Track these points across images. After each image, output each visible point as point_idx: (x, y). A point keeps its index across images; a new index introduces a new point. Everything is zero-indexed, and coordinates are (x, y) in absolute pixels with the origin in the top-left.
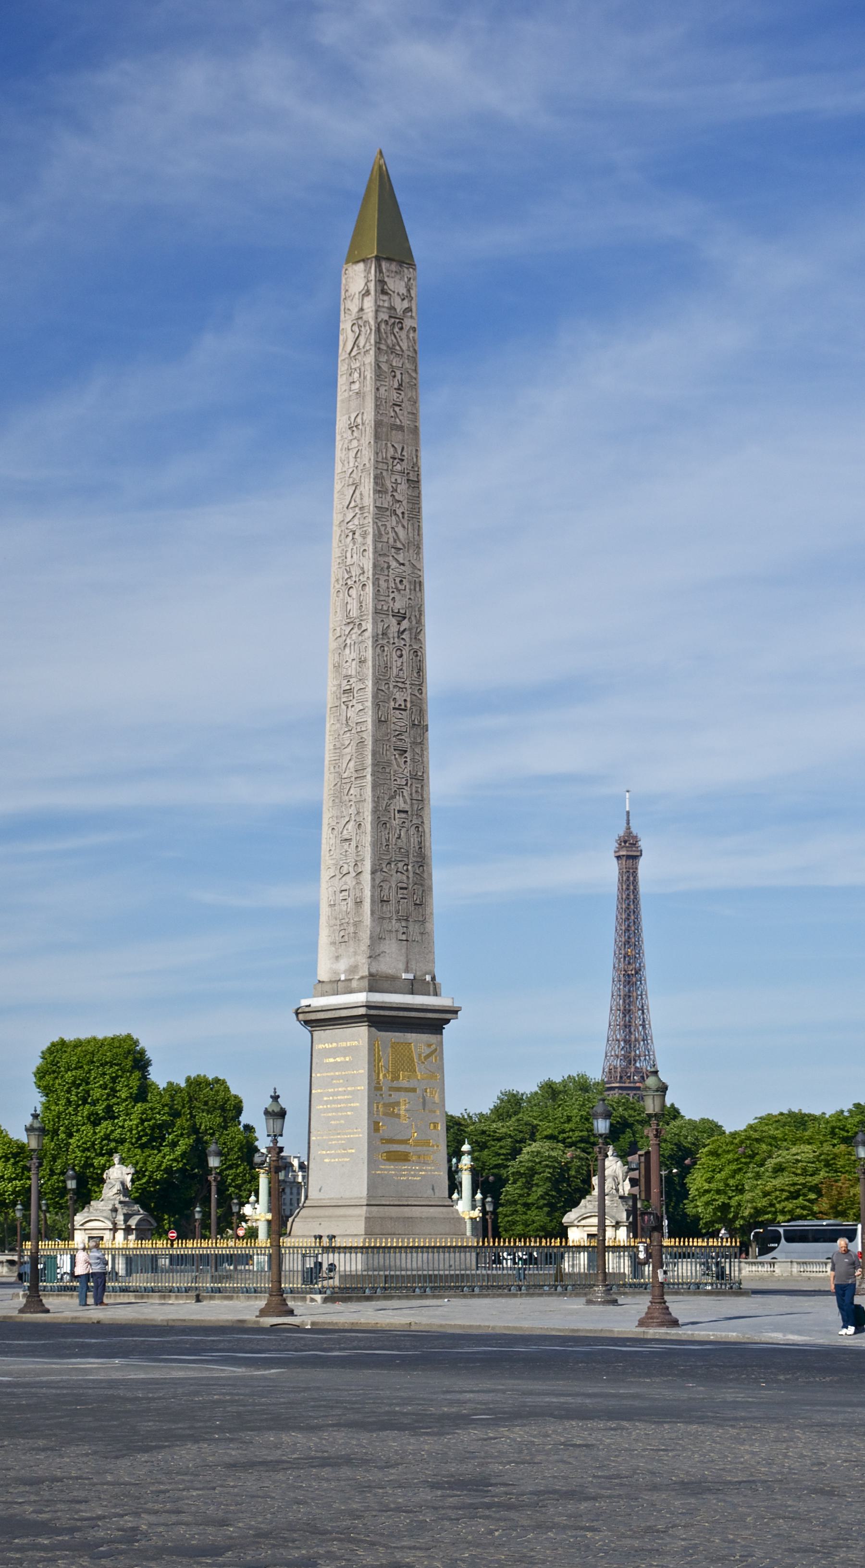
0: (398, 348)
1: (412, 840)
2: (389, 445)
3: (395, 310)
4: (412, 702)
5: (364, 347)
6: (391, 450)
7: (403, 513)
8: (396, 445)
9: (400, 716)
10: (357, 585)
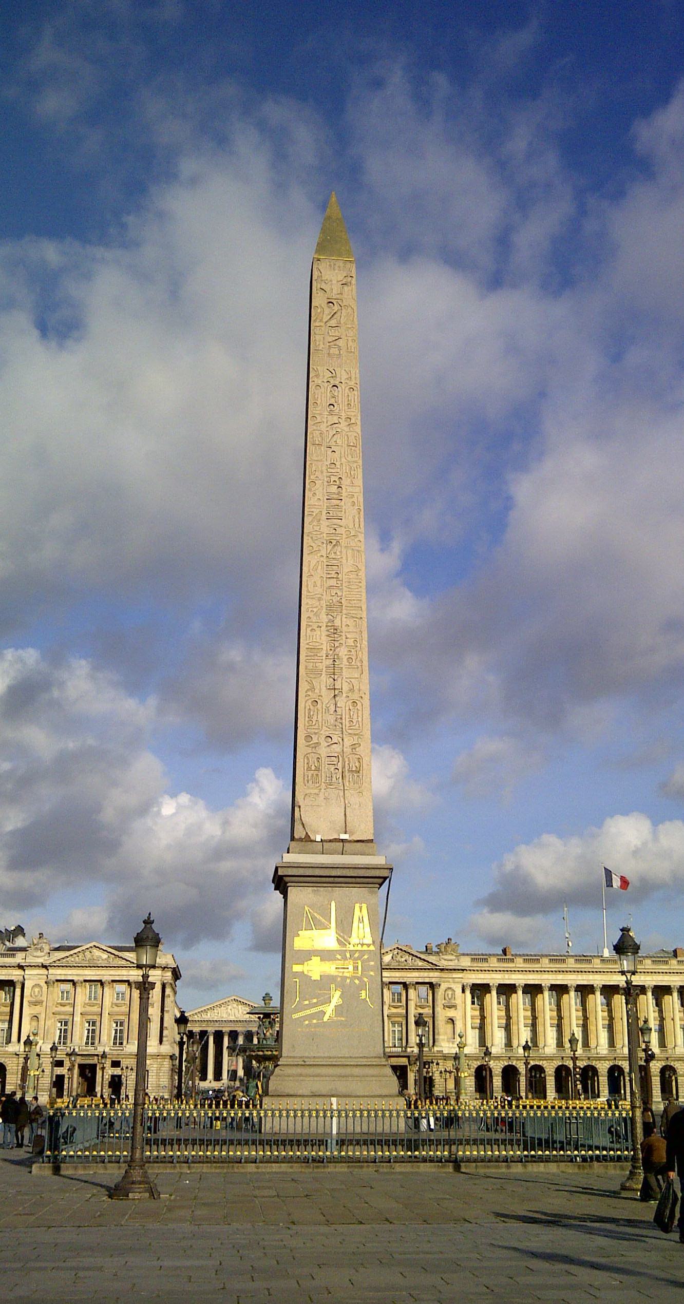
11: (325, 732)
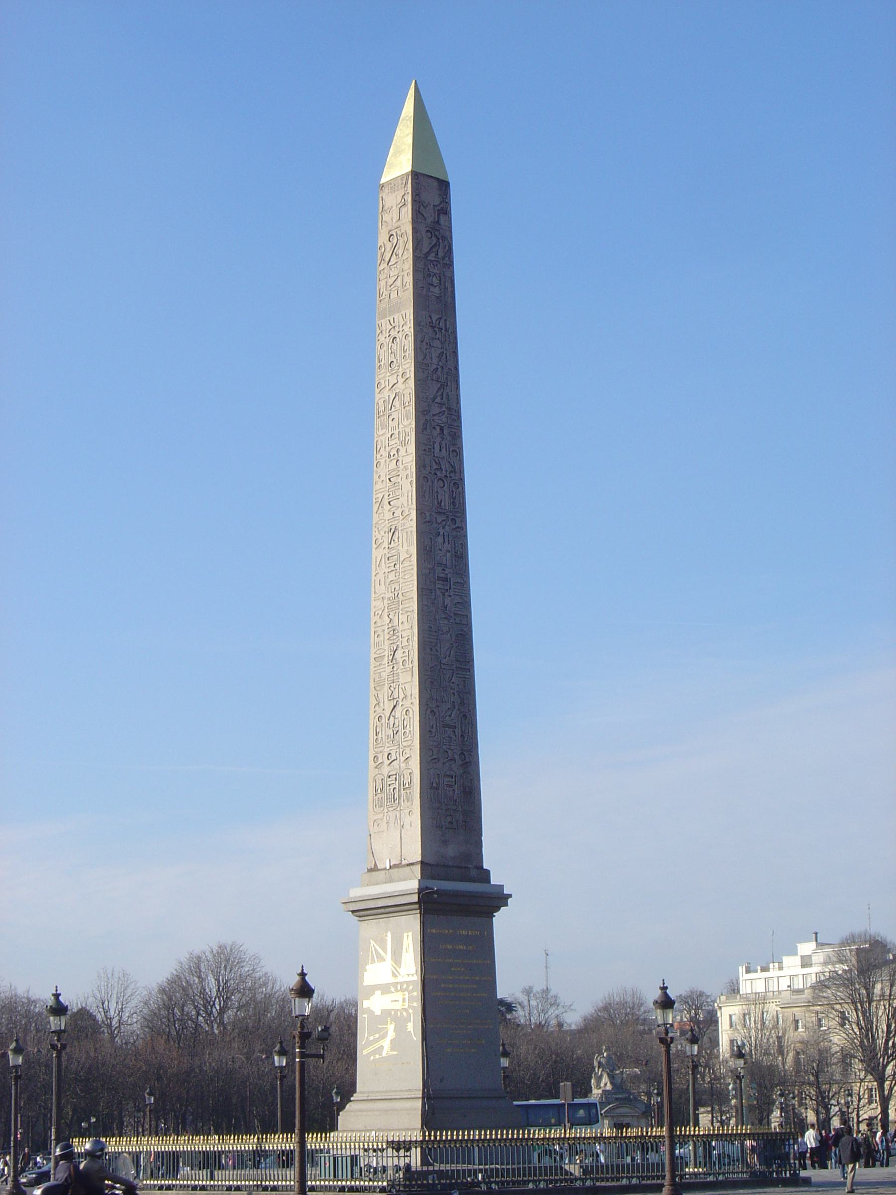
5: (443, 258)
10: (449, 480)
11: (387, 751)
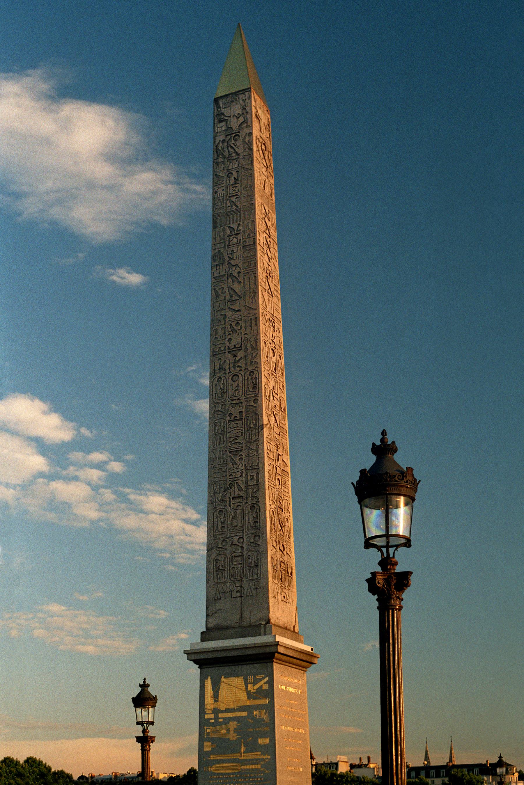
0: (234, 154)
1: (247, 517)
2: (226, 227)
3: (232, 128)
4: (246, 412)
6: (228, 231)
7: (240, 272)
8: (232, 226)
9: (235, 425)
